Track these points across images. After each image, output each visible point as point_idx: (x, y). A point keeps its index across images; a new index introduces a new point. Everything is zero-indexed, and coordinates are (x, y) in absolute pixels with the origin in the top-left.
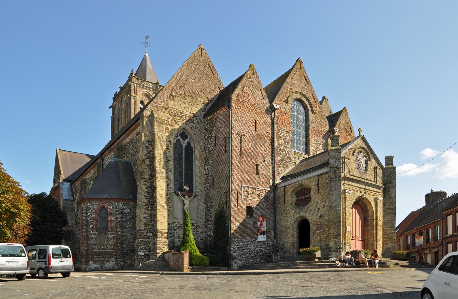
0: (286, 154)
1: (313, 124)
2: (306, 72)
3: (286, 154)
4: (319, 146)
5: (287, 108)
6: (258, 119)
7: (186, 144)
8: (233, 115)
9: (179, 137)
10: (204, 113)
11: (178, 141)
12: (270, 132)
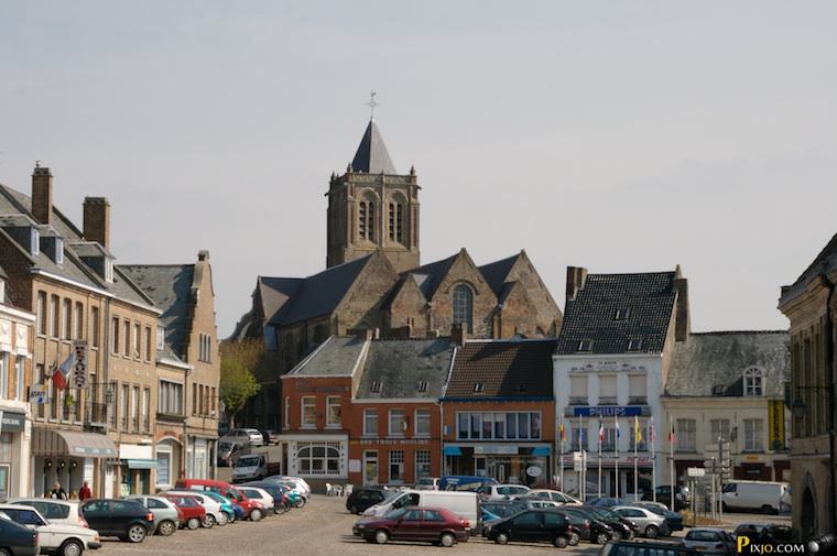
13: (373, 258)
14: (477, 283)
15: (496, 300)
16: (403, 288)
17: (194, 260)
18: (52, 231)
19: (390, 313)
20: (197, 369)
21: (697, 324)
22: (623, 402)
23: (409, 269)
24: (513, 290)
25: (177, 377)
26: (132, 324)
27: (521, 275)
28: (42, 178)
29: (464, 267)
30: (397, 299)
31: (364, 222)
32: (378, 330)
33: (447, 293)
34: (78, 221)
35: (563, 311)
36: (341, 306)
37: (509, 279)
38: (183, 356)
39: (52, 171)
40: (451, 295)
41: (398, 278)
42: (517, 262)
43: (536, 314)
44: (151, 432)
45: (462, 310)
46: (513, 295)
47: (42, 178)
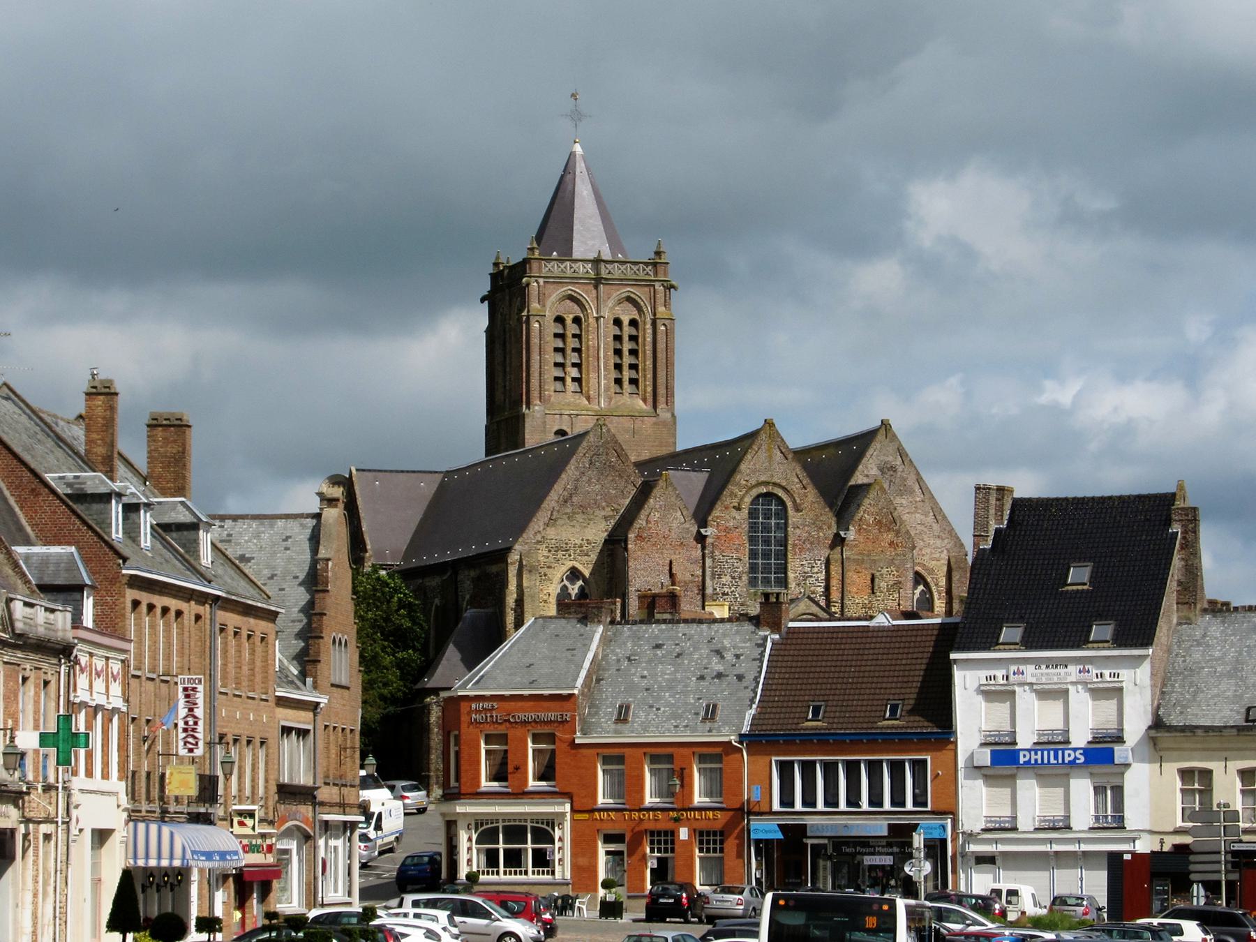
0: (737, 598)
1: (798, 531)
2: (783, 440)
3: (737, 598)
5: (738, 517)
6: (673, 557)
7: (576, 591)
8: (630, 564)
9: (566, 582)
10: (606, 534)
11: (565, 588)
12: (699, 573)
14: (795, 487)
15: (833, 521)
19: (626, 549)
27: (882, 470)
29: (770, 458)
30: (641, 522)
36: (529, 535)
37: (858, 478)
43: (914, 547)
45: (767, 542)
46: (867, 510)
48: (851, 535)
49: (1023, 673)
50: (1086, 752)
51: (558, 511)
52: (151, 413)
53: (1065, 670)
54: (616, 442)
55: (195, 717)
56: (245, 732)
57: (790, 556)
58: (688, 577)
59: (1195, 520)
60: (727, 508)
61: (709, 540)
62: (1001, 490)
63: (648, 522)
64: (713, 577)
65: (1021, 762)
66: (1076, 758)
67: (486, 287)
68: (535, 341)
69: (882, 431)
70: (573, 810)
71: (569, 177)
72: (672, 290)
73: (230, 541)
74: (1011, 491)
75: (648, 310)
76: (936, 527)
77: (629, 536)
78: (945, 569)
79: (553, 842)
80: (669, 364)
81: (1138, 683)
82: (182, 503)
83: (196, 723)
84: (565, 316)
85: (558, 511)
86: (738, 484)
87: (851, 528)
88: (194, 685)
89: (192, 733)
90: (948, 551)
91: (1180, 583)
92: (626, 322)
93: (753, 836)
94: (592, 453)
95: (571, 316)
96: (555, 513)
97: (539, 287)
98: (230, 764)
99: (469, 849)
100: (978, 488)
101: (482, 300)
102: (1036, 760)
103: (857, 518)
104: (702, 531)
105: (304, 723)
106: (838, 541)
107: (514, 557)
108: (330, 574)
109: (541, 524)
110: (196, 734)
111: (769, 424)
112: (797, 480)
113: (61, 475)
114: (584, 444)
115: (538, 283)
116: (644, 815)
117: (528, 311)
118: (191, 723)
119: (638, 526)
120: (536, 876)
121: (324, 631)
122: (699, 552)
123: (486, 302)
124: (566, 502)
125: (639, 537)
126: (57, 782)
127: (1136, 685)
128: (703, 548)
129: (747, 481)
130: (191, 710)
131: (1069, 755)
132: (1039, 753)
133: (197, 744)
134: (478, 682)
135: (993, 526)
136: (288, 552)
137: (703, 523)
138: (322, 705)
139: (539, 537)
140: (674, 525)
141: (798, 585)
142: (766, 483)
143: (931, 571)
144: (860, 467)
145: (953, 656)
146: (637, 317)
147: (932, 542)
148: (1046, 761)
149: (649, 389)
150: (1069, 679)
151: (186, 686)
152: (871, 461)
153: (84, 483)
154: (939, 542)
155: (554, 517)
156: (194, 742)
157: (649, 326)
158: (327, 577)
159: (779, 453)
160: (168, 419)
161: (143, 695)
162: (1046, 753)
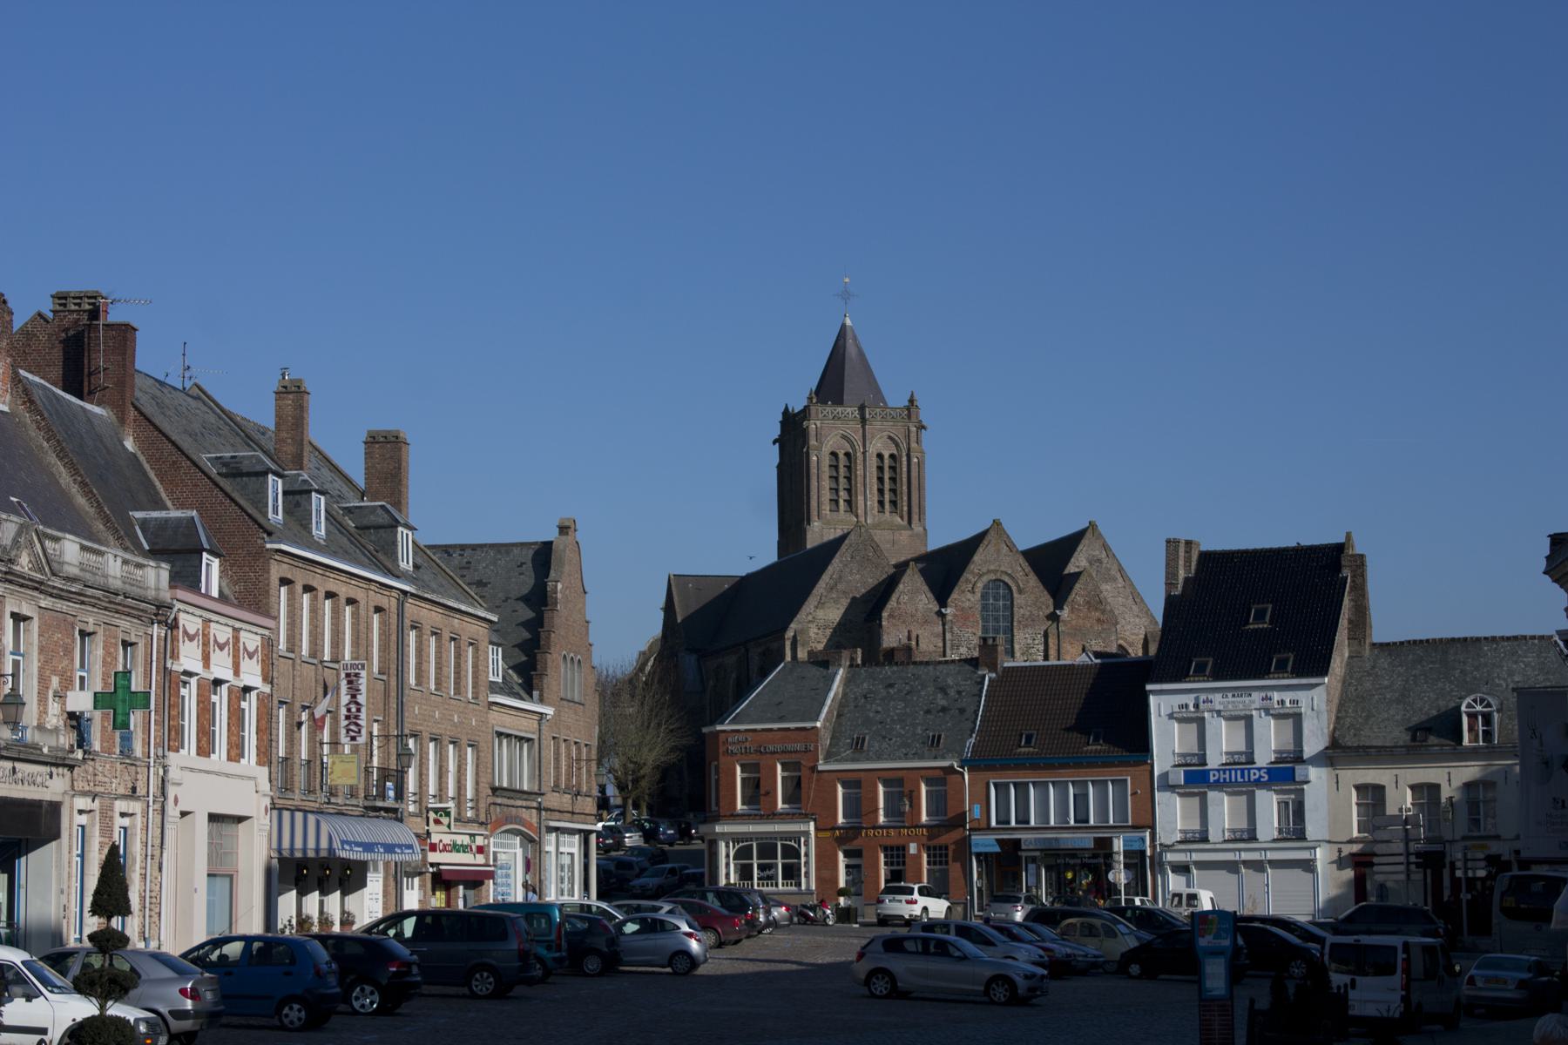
2: (1008, 536)
4: (1034, 639)
5: (972, 599)
6: (920, 632)
8: (884, 637)
12: (941, 644)
13: (852, 537)
14: (1019, 575)
15: (1051, 602)
16: (901, 586)
17: (551, 534)
18: (305, 481)
19: (880, 626)
20: (558, 713)
21: (1383, 629)
22: (1264, 756)
23: (909, 557)
24: (1077, 586)
25: (526, 727)
26: (446, 635)
28: (292, 395)
29: (998, 551)
30: (892, 603)
31: (837, 472)
32: (859, 651)
33: (973, 591)
34: (356, 470)
35: (1160, 620)
36: (802, 615)
37: (1071, 568)
38: (536, 693)
39: (308, 385)
40: (978, 595)
41: (892, 570)
42: (1085, 541)
43: (1117, 623)
44: (482, 818)
45: (996, 619)
46: (1078, 594)
47: (292, 395)
48: (1065, 614)
49: (1211, 702)
50: (1269, 771)
51: (826, 596)
52: (369, 432)
53: (1250, 698)
54: (873, 540)
55: (357, 704)
56: (445, 730)
57: (1015, 631)
58: (932, 648)
59: (1363, 565)
60: (963, 592)
61: (949, 618)
62: (1188, 543)
63: (898, 603)
64: (952, 649)
65: (1211, 781)
66: (1261, 777)
67: (776, 432)
68: (814, 471)
69: (1090, 530)
70: (817, 829)
71: (841, 342)
72: (923, 430)
73: (469, 568)
74: (1198, 545)
75: (904, 446)
76: (1134, 607)
77: (883, 614)
78: (1142, 642)
79: (799, 858)
80: (920, 488)
81: (1315, 708)
82: (382, 507)
83: (359, 710)
84: (838, 451)
85: (826, 596)
86: (972, 572)
87: (1065, 607)
88: (357, 671)
89: (354, 720)
90: (1145, 627)
91: (1350, 622)
92: (886, 456)
93: (974, 850)
94: (853, 550)
95: (843, 452)
96: (823, 598)
97: (817, 428)
98: (408, 757)
99: (728, 865)
100: (1168, 541)
101: (774, 443)
102: (1225, 779)
103: (1070, 599)
104: (943, 610)
105: (530, 732)
106: (1054, 617)
107: (790, 634)
108: (559, 596)
109: (812, 607)
110: (359, 722)
111: (997, 523)
112: (1020, 569)
113: (218, 455)
114: (846, 542)
115: (815, 424)
116: (878, 833)
117: (808, 447)
118: (354, 710)
119: (890, 607)
120: (785, 888)
121: (552, 649)
122: (941, 627)
123: (777, 444)
124: (832, 589)
125: (891, 616)
126: (149, 757)
127: (1313, 709)
128: (944, 625)
129: (979, 570)
130: (354, 696)
131: (1255, 774)
132: (1228, 772)
133: (359, 732)
134: (734, 718)
135: (1182, 574)
136: (522, 577)
137: (943, 602)
138: (548, 717)
139: (810, 618)
140: (920, 606)
141: (1023, 654)
142: (995, 571)
143: (1131, 644)
144: (1073, 560)
145: (1149, 687)
146: (895, 452)
147: (1132, 620)
148: (1233, 780)
149: (905, 508)
150: (1253, 706)
151: (349, 671)
152: (1081, 555)
153: (241, 463)
154: (1137, 620)
155: (822, 601)
156: (356, 730)
157: (904, 459)
158: (556, 598)
159: (1005, 547)
160: (386, 437)
161: (298, 679)
162: (1233, 772)
